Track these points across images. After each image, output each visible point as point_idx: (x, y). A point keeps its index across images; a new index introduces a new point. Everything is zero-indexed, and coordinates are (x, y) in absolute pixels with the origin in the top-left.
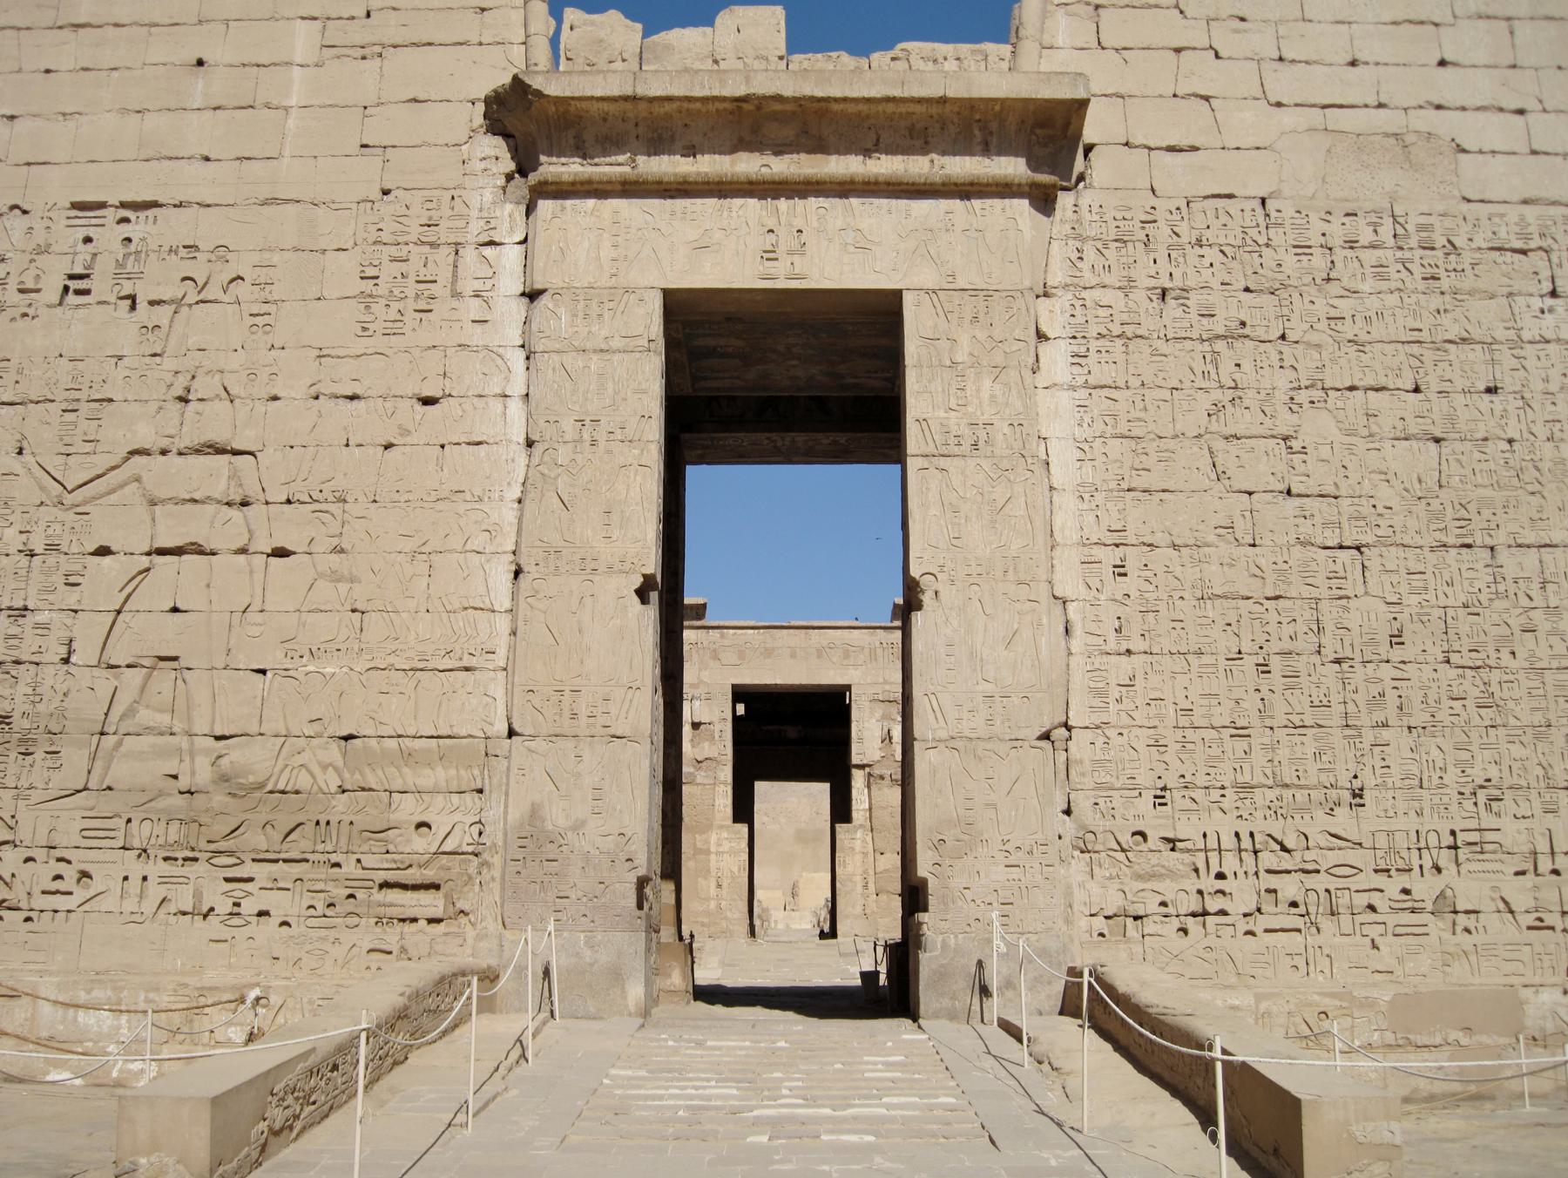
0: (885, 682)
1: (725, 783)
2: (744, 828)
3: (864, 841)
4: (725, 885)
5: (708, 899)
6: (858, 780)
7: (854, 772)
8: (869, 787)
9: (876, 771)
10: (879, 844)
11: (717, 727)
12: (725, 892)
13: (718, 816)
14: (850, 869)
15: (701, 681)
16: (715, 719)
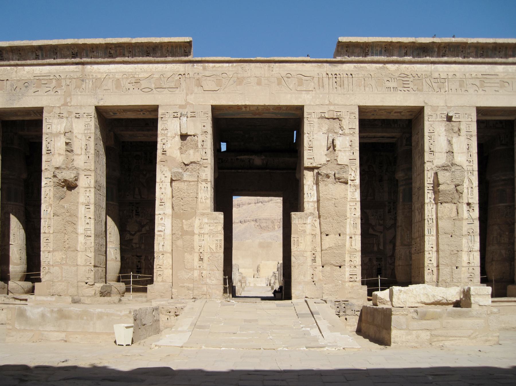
0: (330, 104)
1: (206, 181)
2: (220, 216)
3: (313, 225)
4: (205, 259)
5: (192, 269)
6: (308, 179)
7: (306, 172)
8: (317, 184)
9: (323, 171)
10: (325, 227)
11: (200, 138)
12: (205, 264)
13: (200, 206)
14: (302, 247)
15: (187, 103)
16: (199, 132)
